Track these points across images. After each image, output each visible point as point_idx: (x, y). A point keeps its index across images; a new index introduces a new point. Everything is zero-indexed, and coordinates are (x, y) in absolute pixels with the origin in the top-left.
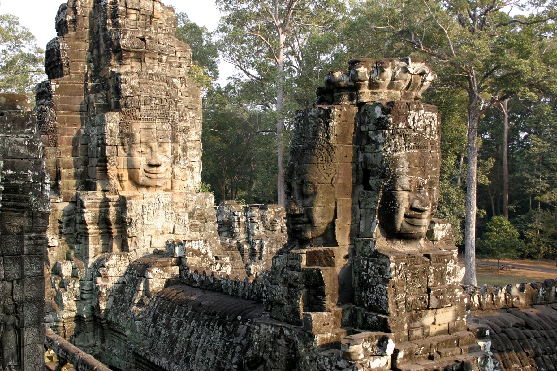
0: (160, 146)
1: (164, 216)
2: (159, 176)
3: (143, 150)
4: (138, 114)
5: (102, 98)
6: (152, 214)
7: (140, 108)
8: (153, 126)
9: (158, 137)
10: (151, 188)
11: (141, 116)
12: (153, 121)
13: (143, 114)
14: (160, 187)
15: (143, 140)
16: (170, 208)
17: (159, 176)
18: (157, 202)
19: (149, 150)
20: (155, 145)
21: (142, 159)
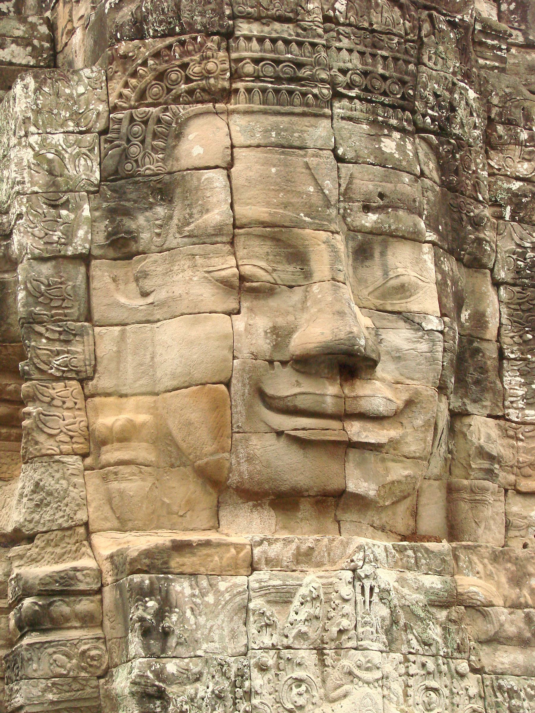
0: (362, 253)
1: (397, 687)
2: (357, 431)
3: (247, 270)
4: (218, 62)
5: (22, 42)
6: (309, 671)
7: (228, 35)
8: (319, 132)
9: (346, 195)
10: (306, 508)
11: (236, 76)
12: (316, 109)
13: (249, 68)
14: (361, 502)
15: (248, 211)
16: (435, 633)
17: (357, 431)
18: (346, 591)
19: (287, 272)
20: (327, 250)
21: (240, 322)
